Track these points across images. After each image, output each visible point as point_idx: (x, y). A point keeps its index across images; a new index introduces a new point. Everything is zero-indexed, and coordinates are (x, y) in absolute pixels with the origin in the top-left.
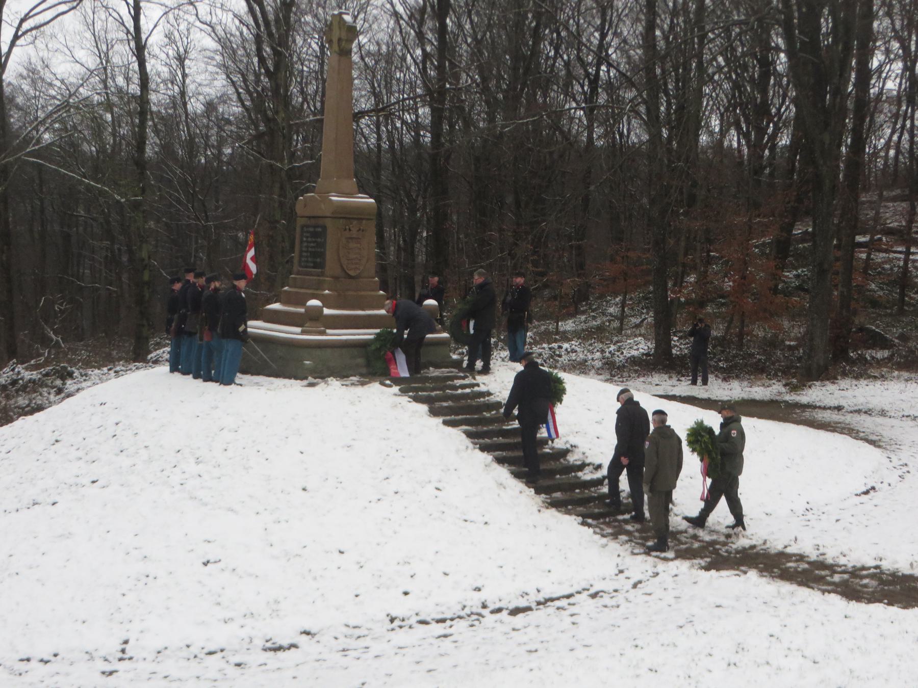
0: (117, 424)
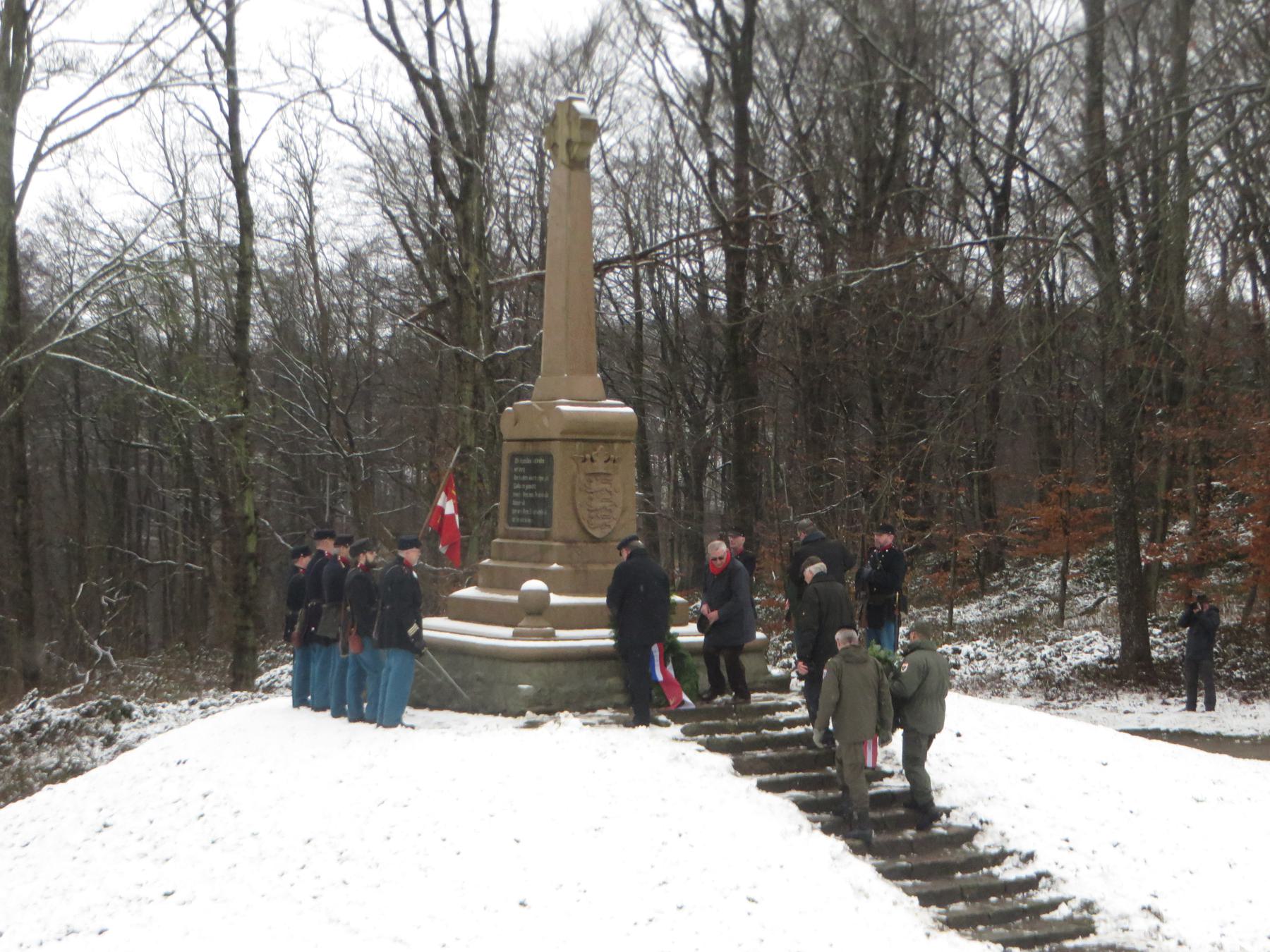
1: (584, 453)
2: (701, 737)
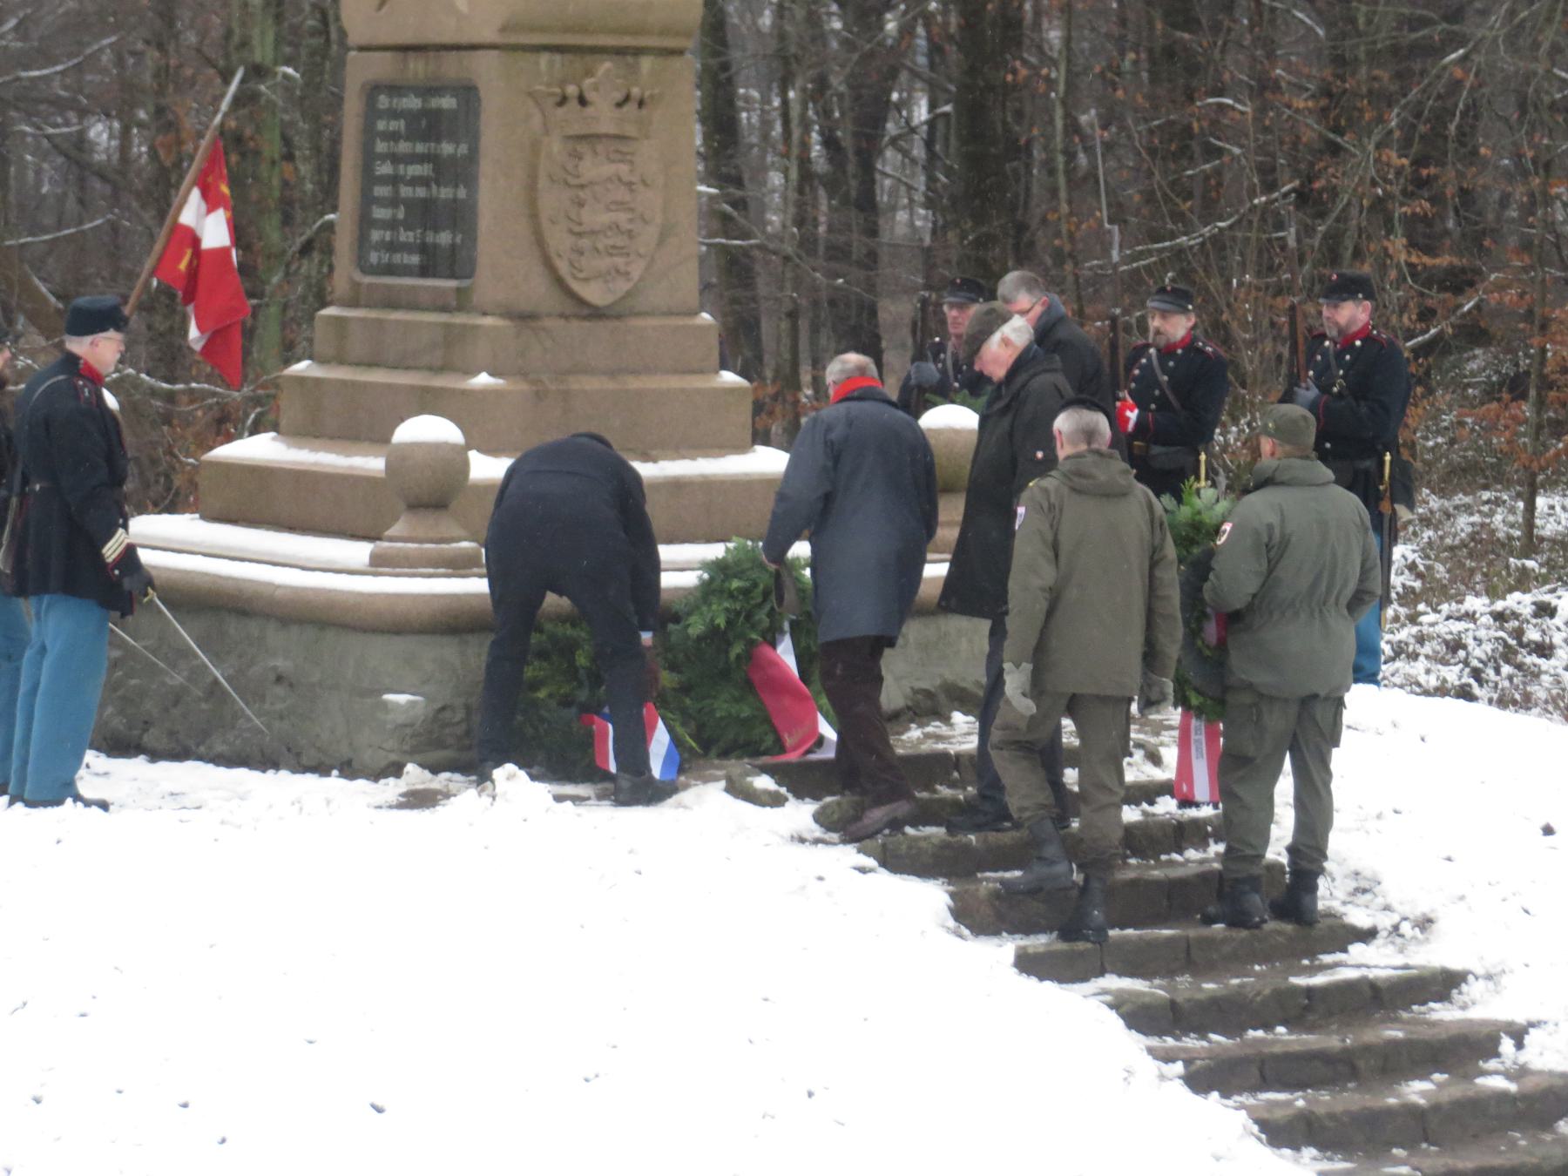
1: (563, 83)
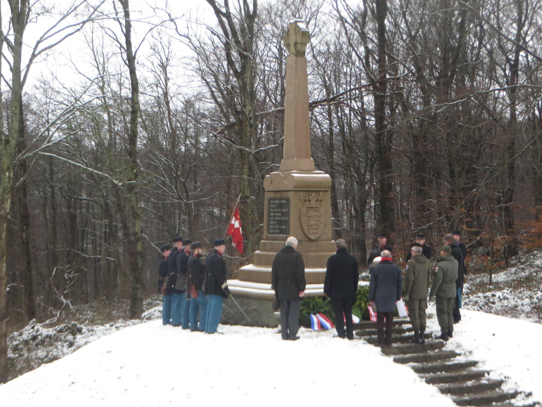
0: (121, 368)
2: (366, 337)
